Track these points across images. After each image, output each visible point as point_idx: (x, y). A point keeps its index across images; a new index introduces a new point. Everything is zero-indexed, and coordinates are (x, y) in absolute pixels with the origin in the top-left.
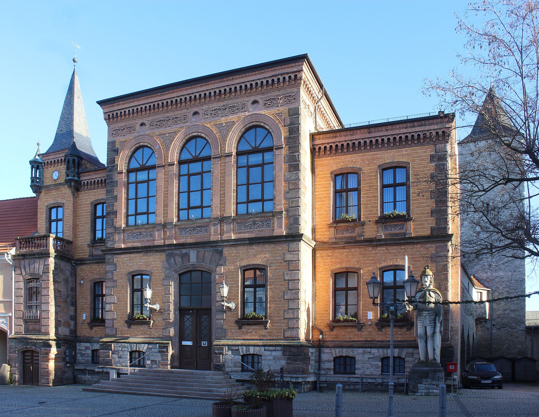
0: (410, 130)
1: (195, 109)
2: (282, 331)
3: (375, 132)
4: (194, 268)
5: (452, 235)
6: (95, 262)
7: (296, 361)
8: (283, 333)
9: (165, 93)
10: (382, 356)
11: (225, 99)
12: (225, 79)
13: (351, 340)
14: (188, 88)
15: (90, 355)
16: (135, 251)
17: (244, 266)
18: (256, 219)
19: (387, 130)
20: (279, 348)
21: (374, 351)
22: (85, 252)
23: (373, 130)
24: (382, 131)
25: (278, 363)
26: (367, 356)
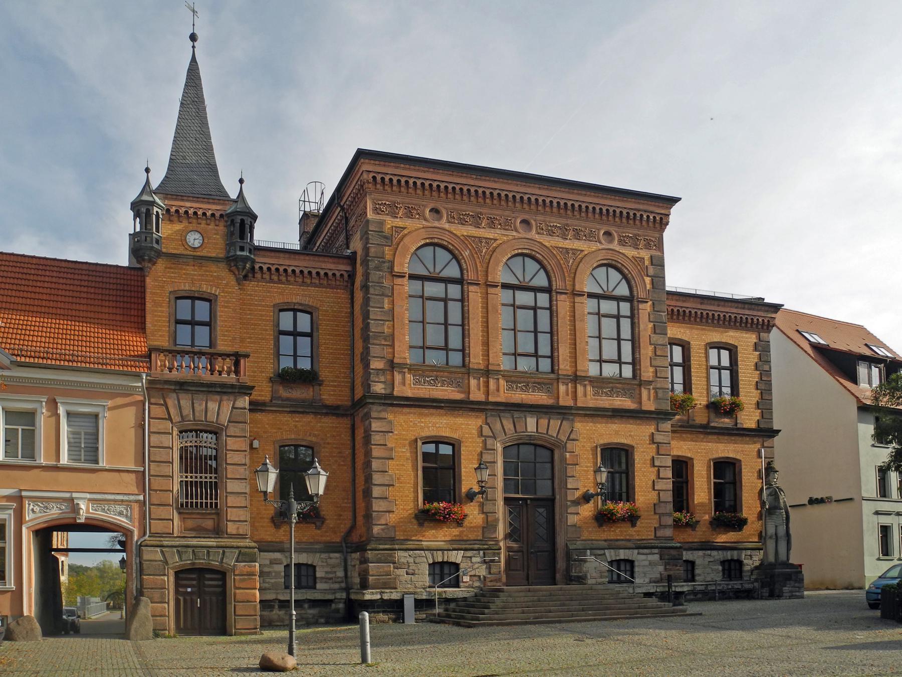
0: (740, 311)
1: (527, 217)
2: (653, 529)
3: (707, 304)
4: (530, 440)
5: (778, 431)
6: (288, 410)
7: (676, 566)
8: (653, 531)
9: (484, 178)
10: (722, 560)
11: (567, 217)
12: (576, 191)
13: (685, 541)
14: (521, 183)
15: (283, 574)
16: (435, 404)
17: (604, 445)
18: (617, 385)
19: (719, 306)
20: (656, 551)
21: (714, 553)
22: (262, 391)
23: (706, 301)
24: (714, 305)
25: (655, 569)
26: (708, 559)
